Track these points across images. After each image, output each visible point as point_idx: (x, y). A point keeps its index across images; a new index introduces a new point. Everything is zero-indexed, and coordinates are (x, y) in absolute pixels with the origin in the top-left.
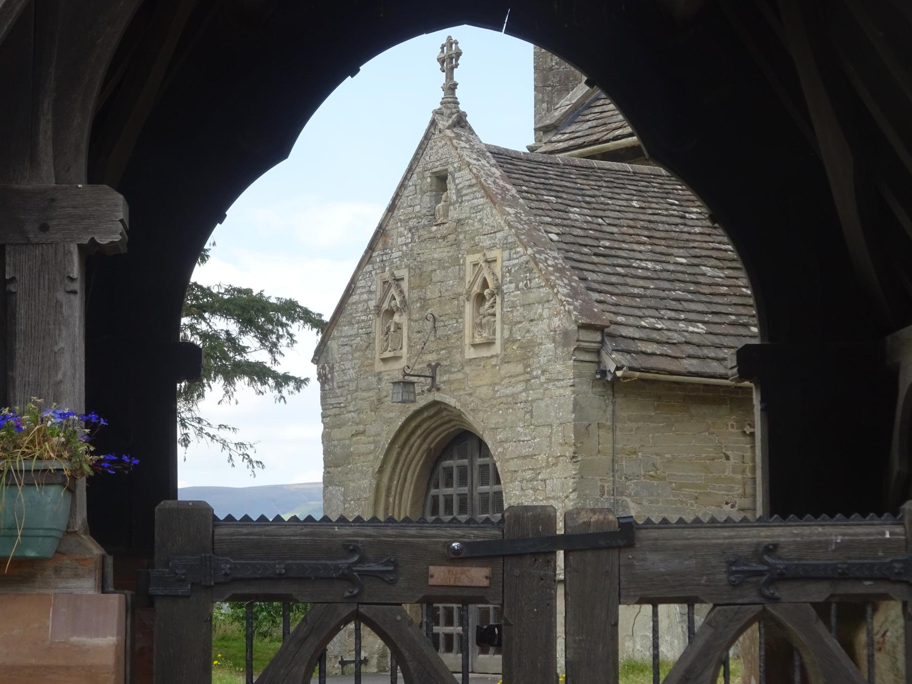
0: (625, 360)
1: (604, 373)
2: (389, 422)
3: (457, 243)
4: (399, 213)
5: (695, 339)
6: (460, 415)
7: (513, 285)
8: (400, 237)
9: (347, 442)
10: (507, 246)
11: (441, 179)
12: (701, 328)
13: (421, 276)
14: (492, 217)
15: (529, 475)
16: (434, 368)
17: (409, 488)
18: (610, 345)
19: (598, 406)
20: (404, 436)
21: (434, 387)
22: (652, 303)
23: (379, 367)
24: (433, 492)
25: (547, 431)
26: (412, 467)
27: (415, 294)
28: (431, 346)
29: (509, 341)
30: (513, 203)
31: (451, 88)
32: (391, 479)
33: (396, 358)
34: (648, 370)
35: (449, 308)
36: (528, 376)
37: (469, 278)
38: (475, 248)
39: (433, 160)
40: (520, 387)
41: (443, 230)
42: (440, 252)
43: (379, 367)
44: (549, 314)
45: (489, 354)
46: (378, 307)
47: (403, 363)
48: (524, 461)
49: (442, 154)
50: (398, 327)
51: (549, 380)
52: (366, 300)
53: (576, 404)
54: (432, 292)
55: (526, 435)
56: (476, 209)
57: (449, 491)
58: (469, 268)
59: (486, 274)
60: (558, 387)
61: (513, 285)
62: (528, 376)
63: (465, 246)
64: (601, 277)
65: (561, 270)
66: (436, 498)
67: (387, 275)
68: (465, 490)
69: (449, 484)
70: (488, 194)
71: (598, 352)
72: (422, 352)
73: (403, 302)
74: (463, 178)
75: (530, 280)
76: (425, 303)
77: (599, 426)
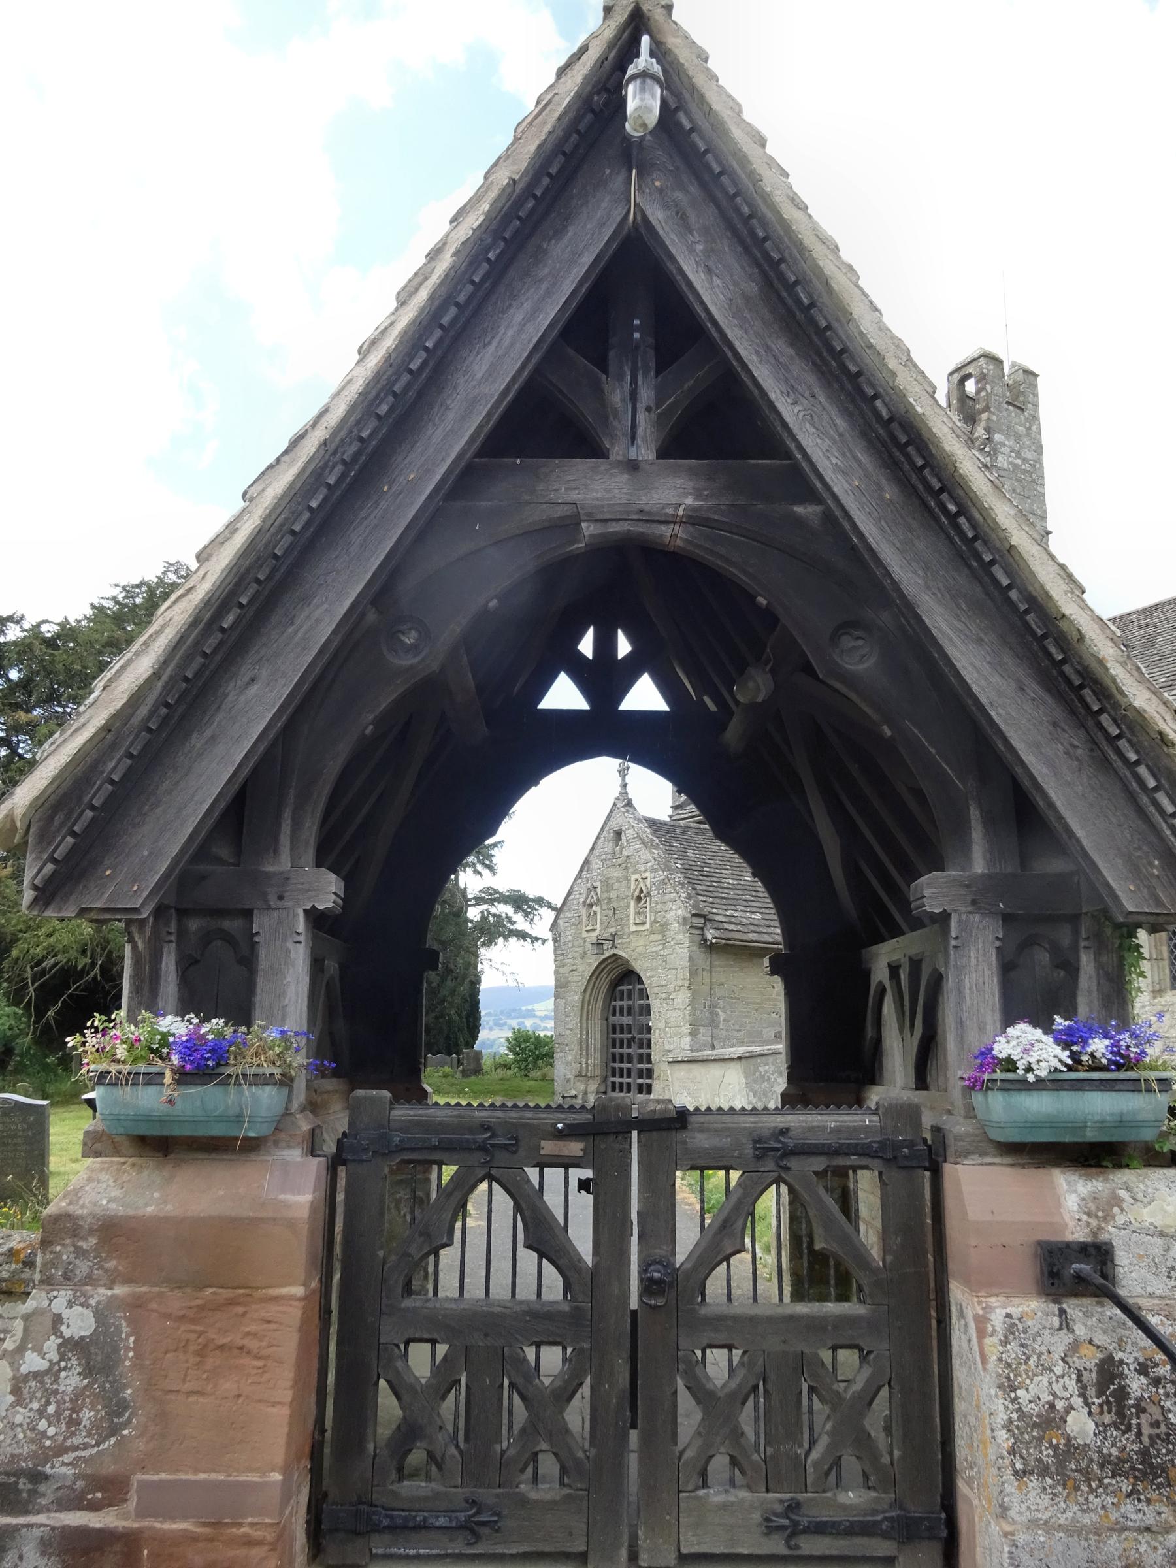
0: (717, 933)
1: (705, 940)
2: (589, 965)
3: (626, 869)
4: (596, 852)
5: (755, 922)
6: (628, 961)
8: (597, 865)
10: (653, 870)
11: (619, 834)
12: (759, 916)
13: (607, 886)
14: (645, 855)
15: (664, 996)
16: (614, 936)
18: (709, 925)
19: (702, 960)
21: (614, 946)
22: (732, 902)
23: (585, 934)
24: (613, 1003)
25: (674, 971)
27: (604, 896)
28: (613, 923)
29: (655, 922)
30: (657, 847)
31: (624, 786)
33: (594, 930)
34: (730, 939)
35: (622, 904)
37: (633, 887)
38: (636, 872)
39: (615, 824)
40: (660, 947)
41: (619, 861)
42: (617, 873)
43: (585, 934)
44: (677, 908)
46: (584, 902)
47: (597, 933)
49: (618, 821)
50: (595, 913)
52: (578, 898)
53: (690, 957)
54: (613, 895)
56: (637, 850)
57: (622, 1003)
58: (633, 882)
59: (642, 885)
60: (680, 948)
63: (631, 870)
64: (704, 888)
65: (682, 884)
66: (615, 1007)
67: (589, 885)
68: (630, 1003)
69: (622, 999)
70: (643, 843)
71: (702, 929)
72: (607, 927)
73: (598, 900)
74: (630, 833)
76: (609, 900)
77: (703, 969)
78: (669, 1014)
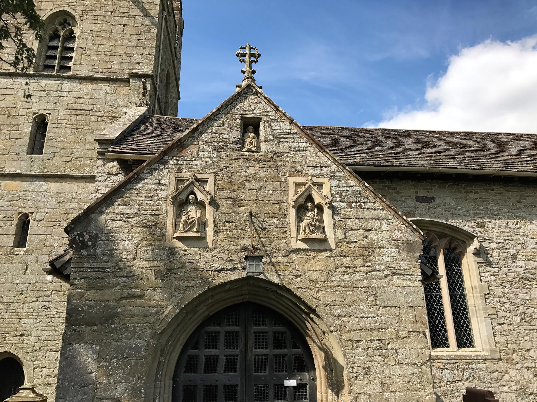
7: (345, 204)
9: (112, 303)
17: (179, 349)
20: (195, 303)
26: (188, 330)
32: (168, 341)
36: (369, 269)
38: (299, 173)
45: (322, 248)
48: (369, 333)
51: (393, 274)
55: (370, 313)
61: (345, 204)
62: (369, 269)
75: (364, 203)
76: (236, 202)
78: (388, 371)
